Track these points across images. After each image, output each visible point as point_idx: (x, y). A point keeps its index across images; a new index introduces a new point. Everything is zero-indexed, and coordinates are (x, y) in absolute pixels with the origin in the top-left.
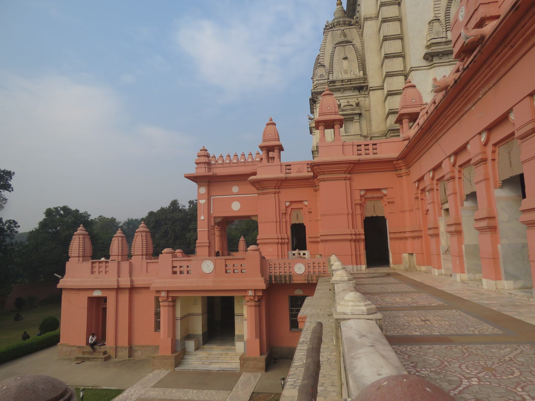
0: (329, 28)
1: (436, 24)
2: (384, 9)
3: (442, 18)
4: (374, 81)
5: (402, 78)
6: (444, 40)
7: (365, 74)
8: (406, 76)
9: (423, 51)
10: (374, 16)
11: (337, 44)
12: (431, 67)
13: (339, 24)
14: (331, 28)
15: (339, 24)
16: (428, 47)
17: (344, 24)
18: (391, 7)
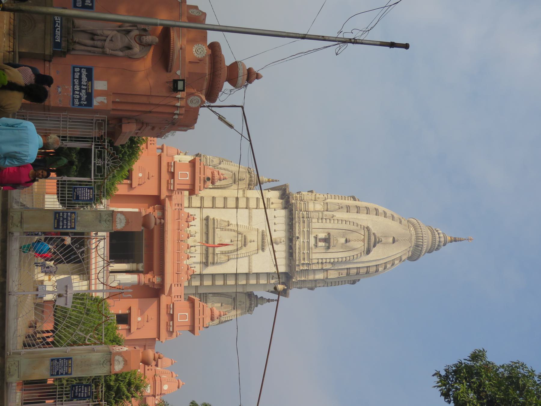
1: (226, 224)
2: (245, 199)
3: (230, 227)
5: (199, 205)
6: (216, 226)
7: (210, 188)
8: (200, 208)
9: (211, 217)
10: (245, 195)
11: (234, 174)
12: (201, 220)
13: (251, 177)
14: (249, 172)
15: (251, 177)
16: (214, 219)
17: (251, 181)
18: (245, 203)
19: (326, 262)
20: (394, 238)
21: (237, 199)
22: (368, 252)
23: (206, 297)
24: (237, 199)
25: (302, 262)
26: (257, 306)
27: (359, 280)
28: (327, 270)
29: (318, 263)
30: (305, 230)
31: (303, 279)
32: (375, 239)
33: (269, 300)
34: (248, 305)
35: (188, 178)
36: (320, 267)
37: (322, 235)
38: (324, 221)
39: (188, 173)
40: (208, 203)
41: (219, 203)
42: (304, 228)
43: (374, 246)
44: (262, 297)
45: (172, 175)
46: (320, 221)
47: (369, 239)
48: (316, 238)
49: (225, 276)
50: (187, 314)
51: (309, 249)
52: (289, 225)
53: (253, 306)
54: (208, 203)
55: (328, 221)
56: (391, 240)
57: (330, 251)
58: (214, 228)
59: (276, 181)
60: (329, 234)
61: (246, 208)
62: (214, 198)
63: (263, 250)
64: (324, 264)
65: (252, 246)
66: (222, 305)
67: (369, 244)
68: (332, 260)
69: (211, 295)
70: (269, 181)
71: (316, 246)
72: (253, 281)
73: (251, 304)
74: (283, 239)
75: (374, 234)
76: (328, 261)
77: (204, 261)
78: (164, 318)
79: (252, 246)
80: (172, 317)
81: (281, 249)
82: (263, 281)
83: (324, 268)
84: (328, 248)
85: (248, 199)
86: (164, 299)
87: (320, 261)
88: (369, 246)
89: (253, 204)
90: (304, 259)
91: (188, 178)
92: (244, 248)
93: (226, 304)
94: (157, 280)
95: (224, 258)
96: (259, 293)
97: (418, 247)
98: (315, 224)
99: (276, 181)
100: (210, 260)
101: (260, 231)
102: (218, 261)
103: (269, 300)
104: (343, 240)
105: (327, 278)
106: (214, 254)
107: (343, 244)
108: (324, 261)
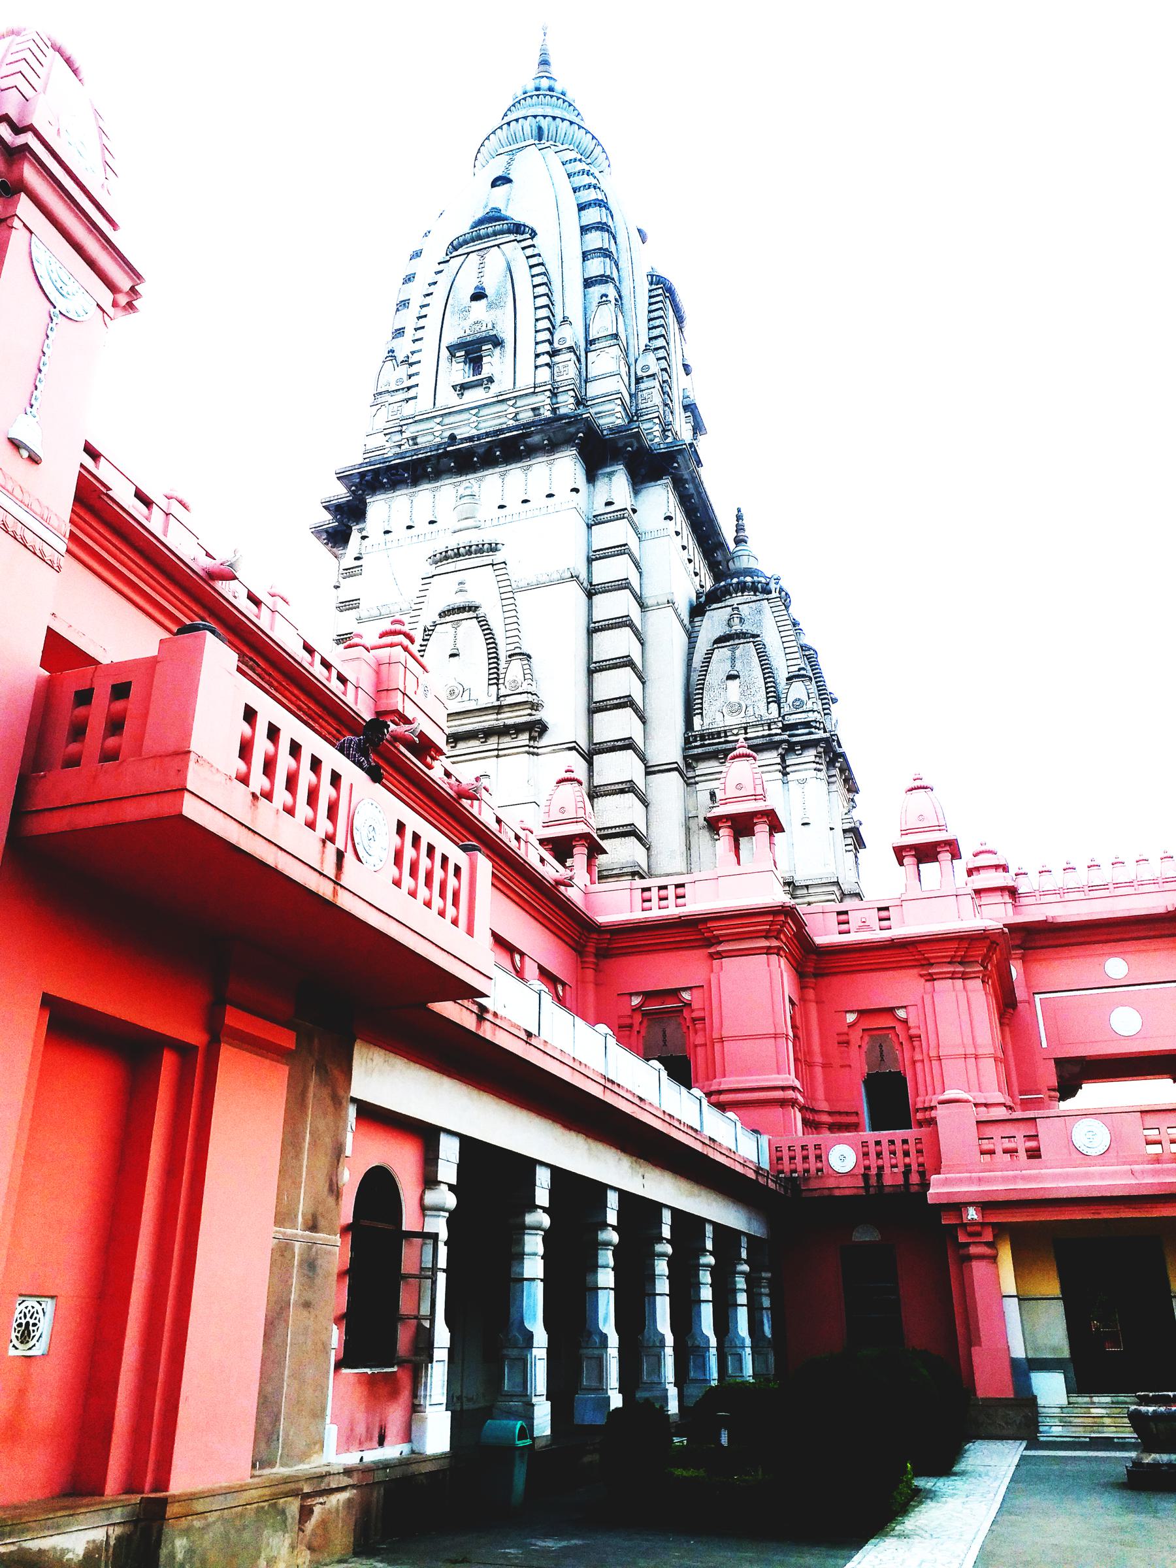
19: (551, 343)
23: (703, 737)
28: (590, 342)
34: (748, 596)
37: (459, 372)
46: (412, 393)
47: (480, 238)
48: (463, 388)
52: (415, 482)
53: (748, 579)
57: (507, 336)
63: (493, 548)
64: (556, 345)
65: (480, 585)
66: (731, 677)
67: (495, 234)
69: (697, 720)
73: (742, 588)
74: (461, 490)
76: (545, 335)
77: (524, 738)
79: (480, 585)
84: (497, 342)
87: (545, 359)
88: (502, 232)
92: (480, 612)
93: (733, 666)
95: (514, 672)
97: (540, 129)
98: (423, 404)
100: (520, 717)
101: (432, 570)
102: (525, 688)
105: (616, 336)
106: (499, 709)
107: (490, 306)
108: (546, 347)
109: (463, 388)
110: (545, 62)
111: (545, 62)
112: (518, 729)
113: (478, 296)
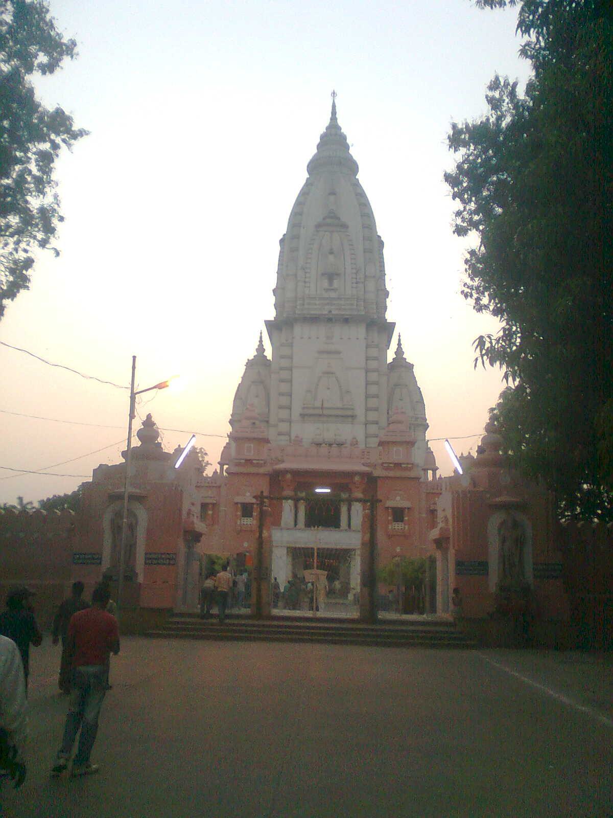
0: (250, 364)
4: (272, 420)
8: (290, 422)
11: (253, 382)
16: (304, 408)
19: (356, 278)
20: (330, 194)
21: (282, 381)
22: (344, 226)
24: (282, 381)
25: (355, 307)
26: (405, 359)
27: (379, 237)
28: (366, 276)
29: (356, 288)
30: (317, 302)
31: (375, 307)
32: (332, 218)
33: (399, 344)
35: (252, 445)
36: (361, 285)
37: (326, 284)
38: (307, 280)
39: (246, 445)
40: (284, 414)
41: (284, 401)
42: (316, 304)
43: (338, 219)
44: (395, 353)
45: (249, 462)
46: (308, 285)
48: (327, 290)
49: (367, 396)
50: (395, 449)
51: (339, 299)
54: (284, 414)
55: (308, 275)
56: (332, 198)
58: (314, 408)
59: (261, 333)
60: (323, 274)
61: (291, 370)
62: (281, 407)
63: (339, 353)
64: (358, 280)
68: (354, 271)
70: (261, 341)
71: (334, 290)
72: (373, 364)
75: (324, 219)
76: (354, 276)
77: (350, 419)
78: (398, 474)
80: (398, 465)
81: (338, 330)
82: (373, 352)
83: (363, 280)
84: (338, 275)
85: (281, 369)
86: (378, 472)
87: (355, 285)
89: (285, 363)
90: (352, 305)
91: (252, 445)
94: (357, 478)
96: (391, 356)
99: (261, 333)
100: (349, 413)
103: (399, 344)
104: (331, 258)
105: (374, 277)
106: (342, 409)
108: (354, 281)
109: (327, 290)
110: (334, 113)
111: (334, 113)
112: (347, 416)
113: (331, 253)
